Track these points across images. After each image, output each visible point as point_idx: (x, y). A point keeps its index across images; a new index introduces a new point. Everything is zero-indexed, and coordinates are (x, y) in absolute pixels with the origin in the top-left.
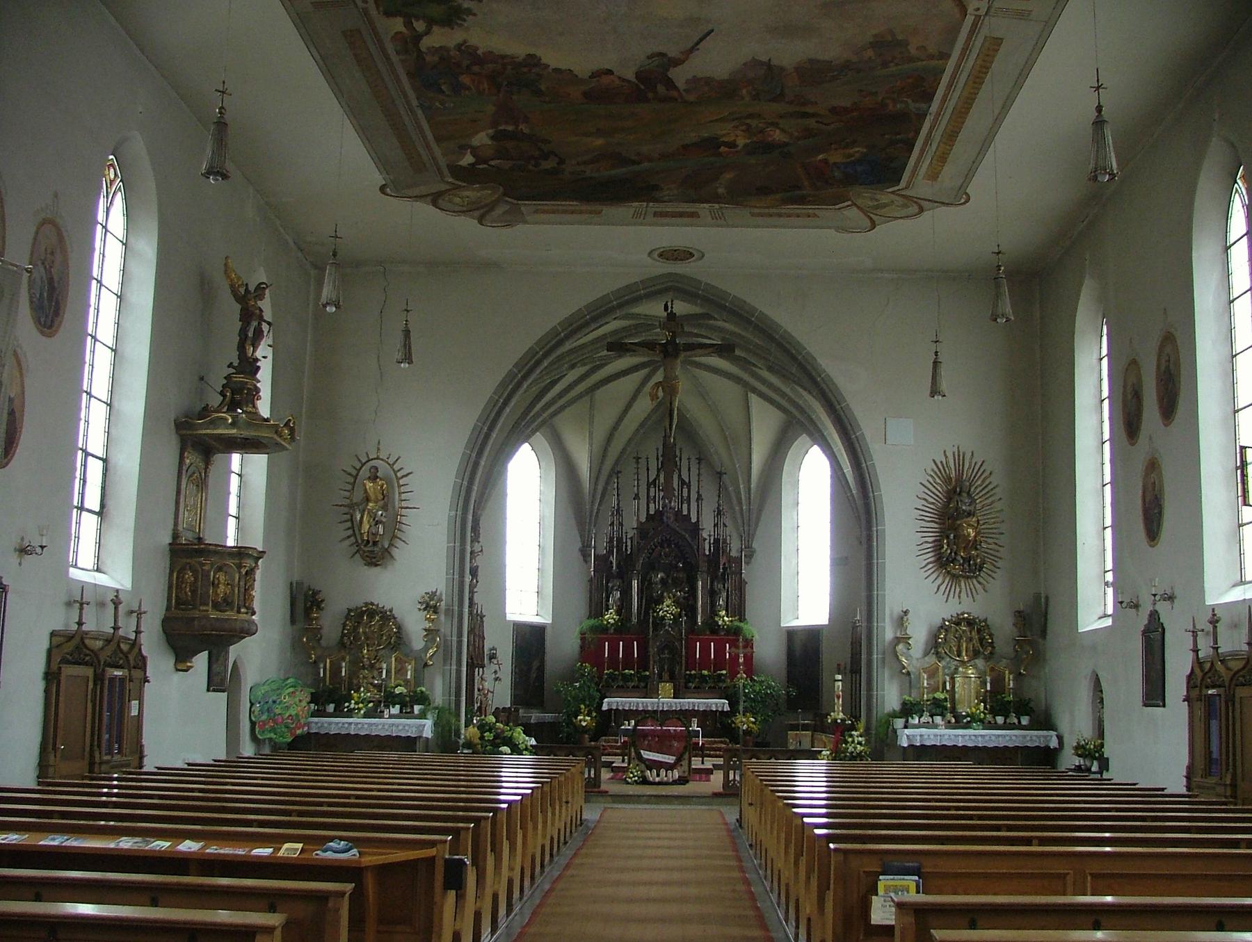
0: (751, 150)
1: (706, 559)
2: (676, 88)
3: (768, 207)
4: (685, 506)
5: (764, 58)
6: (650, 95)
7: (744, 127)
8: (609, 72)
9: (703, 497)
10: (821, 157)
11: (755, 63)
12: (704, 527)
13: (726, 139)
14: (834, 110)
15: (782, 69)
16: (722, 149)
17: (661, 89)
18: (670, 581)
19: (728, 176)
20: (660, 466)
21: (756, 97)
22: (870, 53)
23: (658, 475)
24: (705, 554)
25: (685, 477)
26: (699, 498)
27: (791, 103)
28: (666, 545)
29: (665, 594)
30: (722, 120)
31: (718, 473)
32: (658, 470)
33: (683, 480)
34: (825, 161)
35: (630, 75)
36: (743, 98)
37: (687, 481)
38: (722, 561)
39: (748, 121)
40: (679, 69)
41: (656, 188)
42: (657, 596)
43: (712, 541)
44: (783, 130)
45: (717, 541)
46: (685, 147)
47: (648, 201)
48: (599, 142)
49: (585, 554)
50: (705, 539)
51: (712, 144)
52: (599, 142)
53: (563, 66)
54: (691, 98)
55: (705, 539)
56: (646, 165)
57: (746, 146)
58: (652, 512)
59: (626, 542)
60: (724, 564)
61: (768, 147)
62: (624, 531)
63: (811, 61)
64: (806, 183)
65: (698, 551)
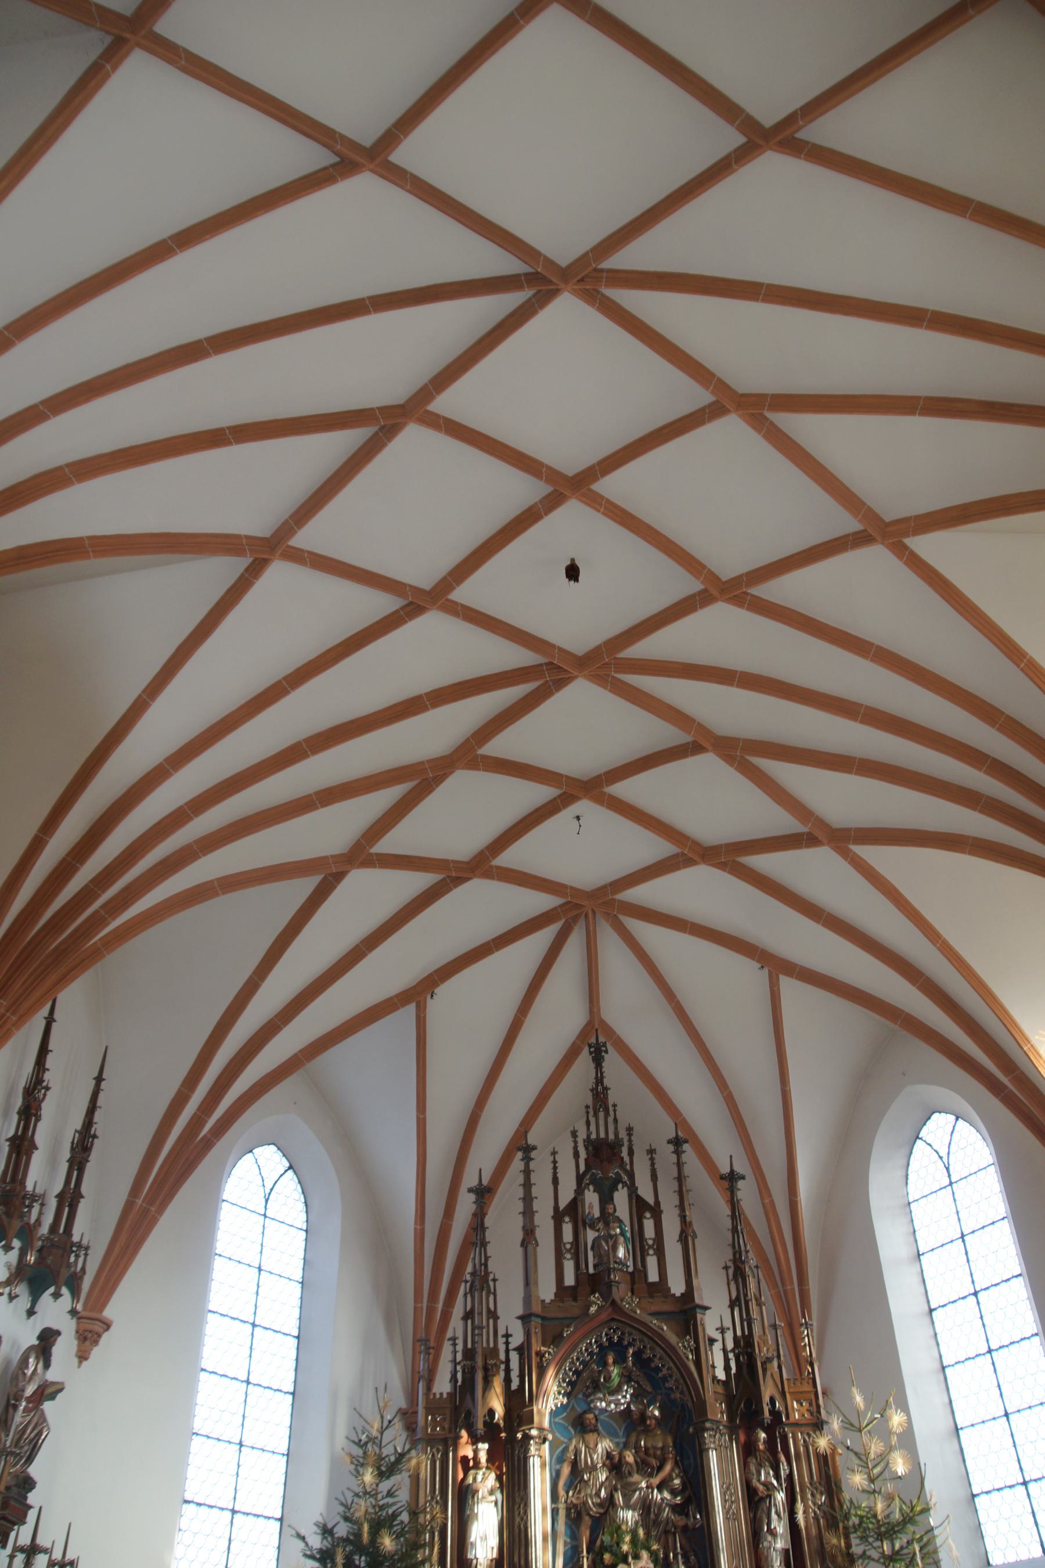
1: (720, 1389)
4: (652, 1262)
9: (696, 1227)
12: (706, 1303)
18: (630, 1457)
20: (582, 1168)
23: (579, 1191)
24: (714, 1378)
25: (646, 1192)
26: (685, 1237)
28: (610, 1360)
29: (619, 1498)
31: (722, 1177)
32: (580, 1178)
33: (639, 1198)
37: (651, 1200)
38: (768, 1390)
42: (600, 1505)
43: (730, 1345)
45: (745, 1346)
49: (408, 1416)
50: (712, 1341)
55: (712, 1341)
58: (570, 1280)
59: (507, 1361)
60: (772, 1401)
62: (501, 1331)
65: (698, 1363)
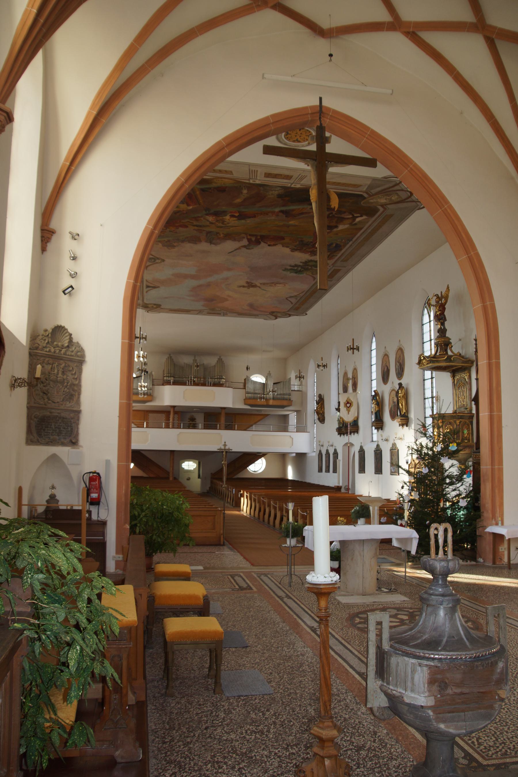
0: (224, 213)
2: (248, 239)
3: (221, 178)
5: (213, 245)
6: (259, 237)
7: (225, 223)
8: (269, 245)
10: (191, 207)
11: (215, 244)
13: (235, 219)
14: (187, 227)
15: (206, 241)
16: (237, 215)
17: (253, 239)
19: (238, 201)
21: (217, 233)
22: (175, 244)
27: (204, 230)
30: (233, 227)
34: (188, 205)
35: (262, 244)
36: (223, 234)
39: (223, 225)
40: (243, 245)
41: (279, 196)
44: (208, 221)
46: (255, 217)
47: (290, 188)
48: (292, 222)
51: (242, 216)
52: (292, 222)
53: (285, 248)
54: (243, 235)
56: (277, 210)
57: (226, 215)
61: (216, 214)
63: (196, 244)
64: (198, 193)
